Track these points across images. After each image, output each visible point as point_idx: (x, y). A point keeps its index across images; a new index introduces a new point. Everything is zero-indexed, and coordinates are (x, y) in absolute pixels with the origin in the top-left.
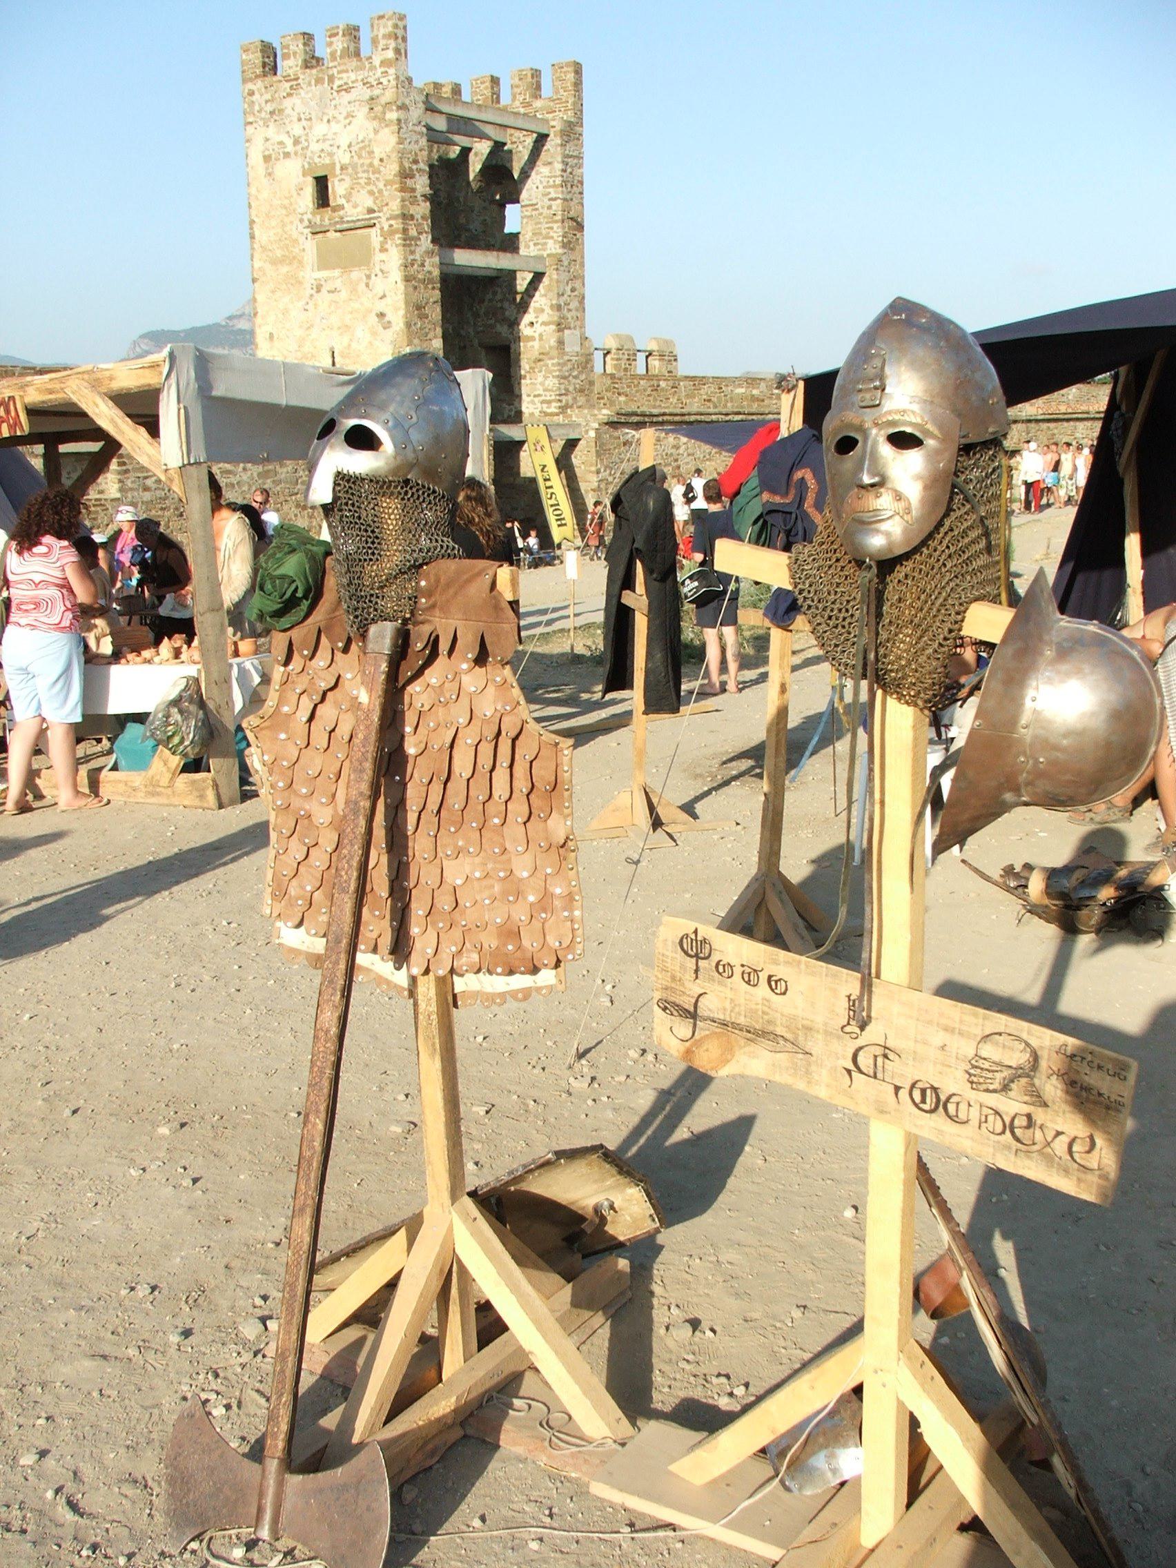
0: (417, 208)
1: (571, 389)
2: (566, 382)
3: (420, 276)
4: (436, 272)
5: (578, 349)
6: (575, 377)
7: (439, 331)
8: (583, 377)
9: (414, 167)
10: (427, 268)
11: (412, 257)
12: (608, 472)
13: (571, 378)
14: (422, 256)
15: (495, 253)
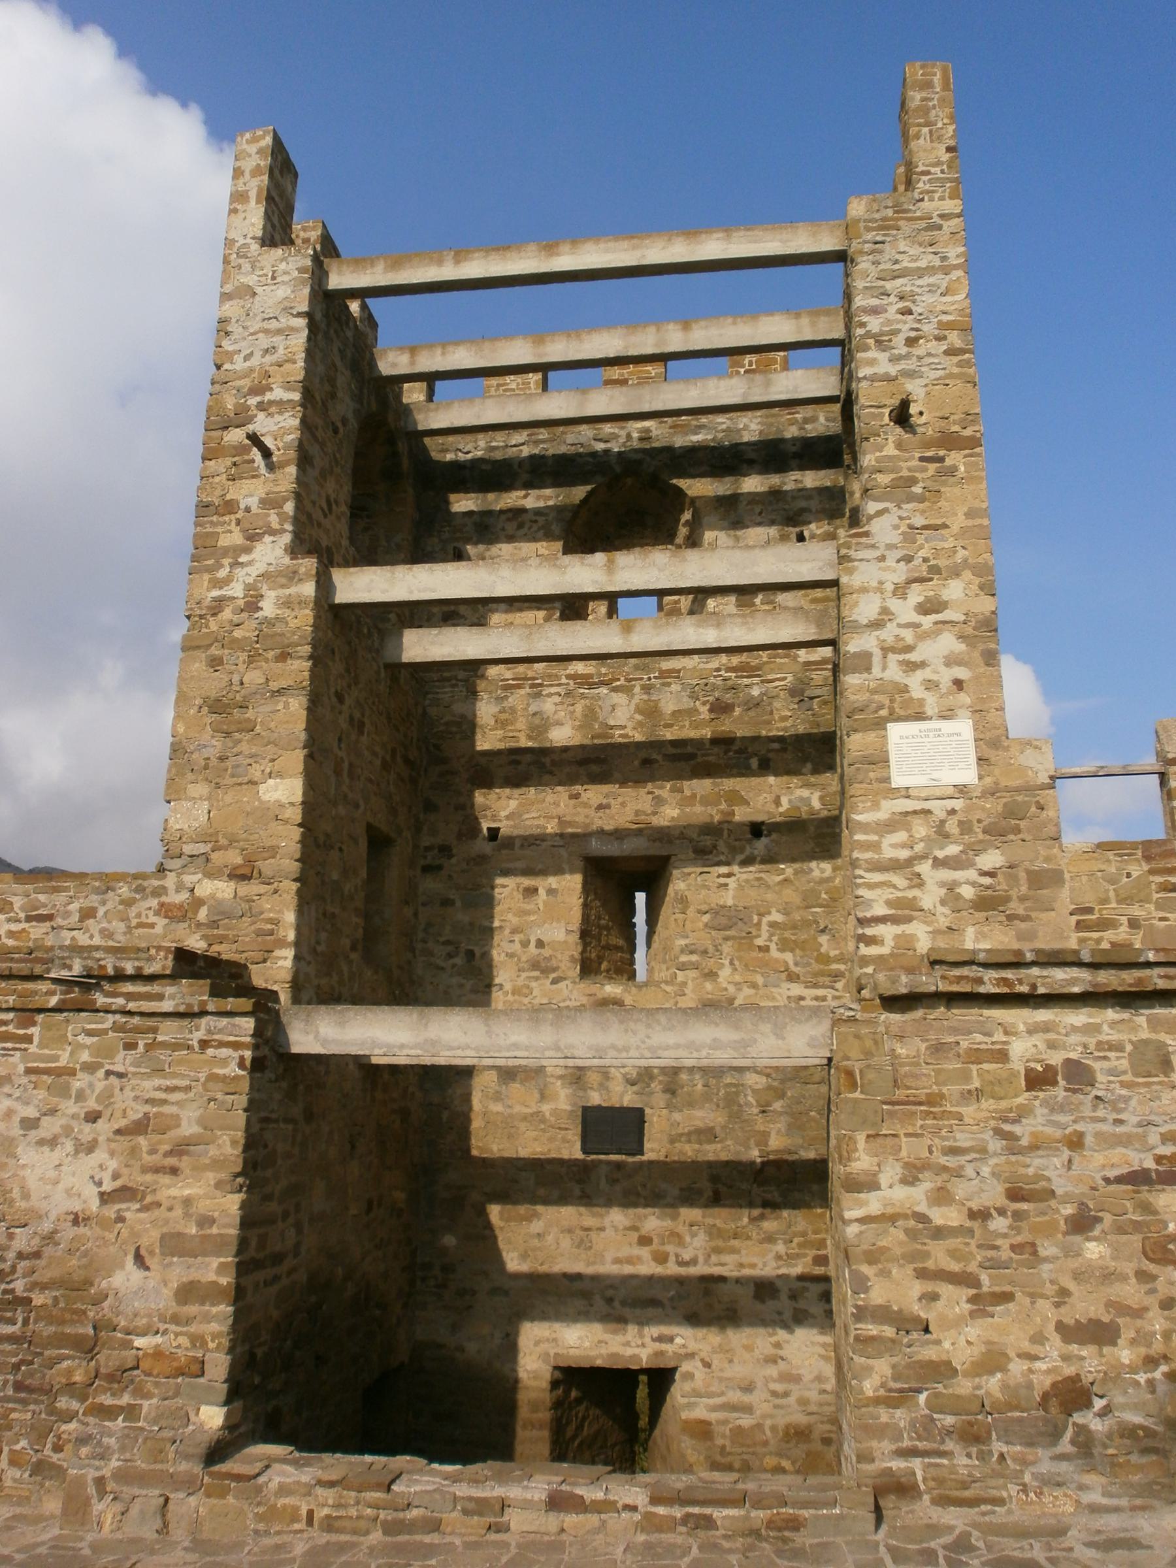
0: (246, 485)
1: (929, 898)
2: (898, 880)
3: (238, 633)
4: (303, 620)
5: (968, 775)
6: (938, 863)
7: (296, 759)
8: (991, 859)
9: (253, 401)
10: (268, 608)
11: (216, 593)
12: (926, 1186)
13: (924, 868)
14: (248, 588)
15: (600, 557)
